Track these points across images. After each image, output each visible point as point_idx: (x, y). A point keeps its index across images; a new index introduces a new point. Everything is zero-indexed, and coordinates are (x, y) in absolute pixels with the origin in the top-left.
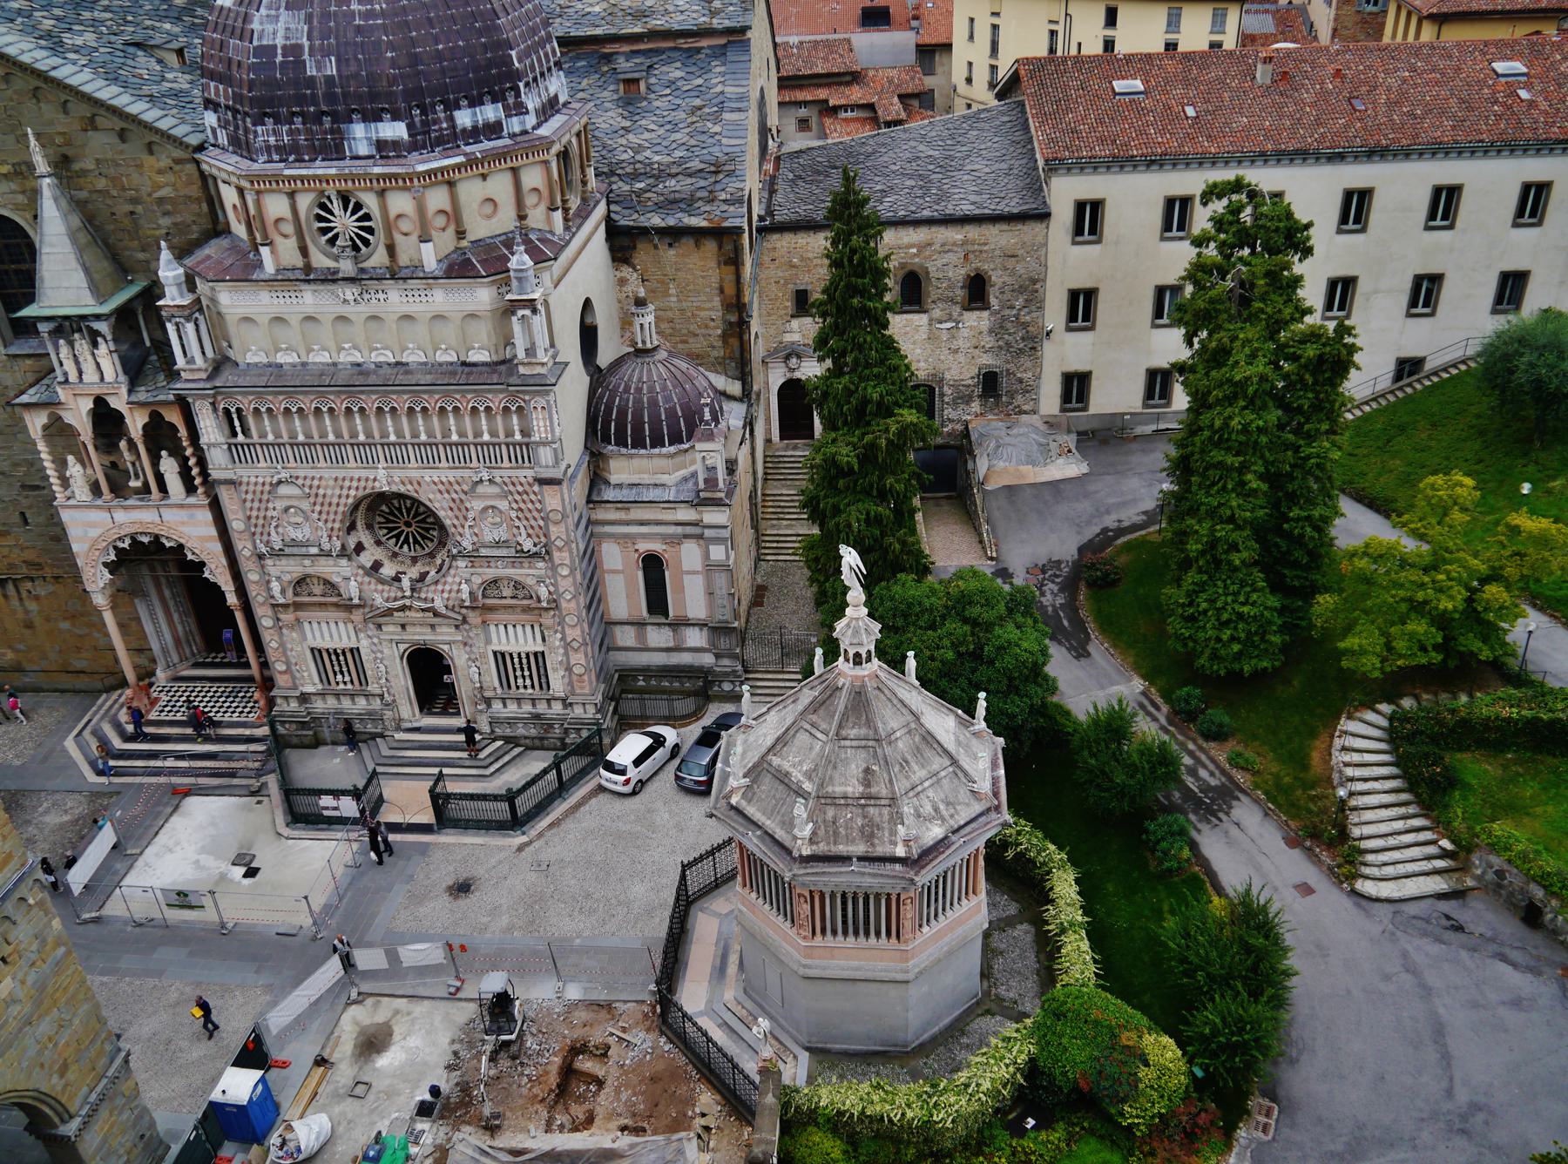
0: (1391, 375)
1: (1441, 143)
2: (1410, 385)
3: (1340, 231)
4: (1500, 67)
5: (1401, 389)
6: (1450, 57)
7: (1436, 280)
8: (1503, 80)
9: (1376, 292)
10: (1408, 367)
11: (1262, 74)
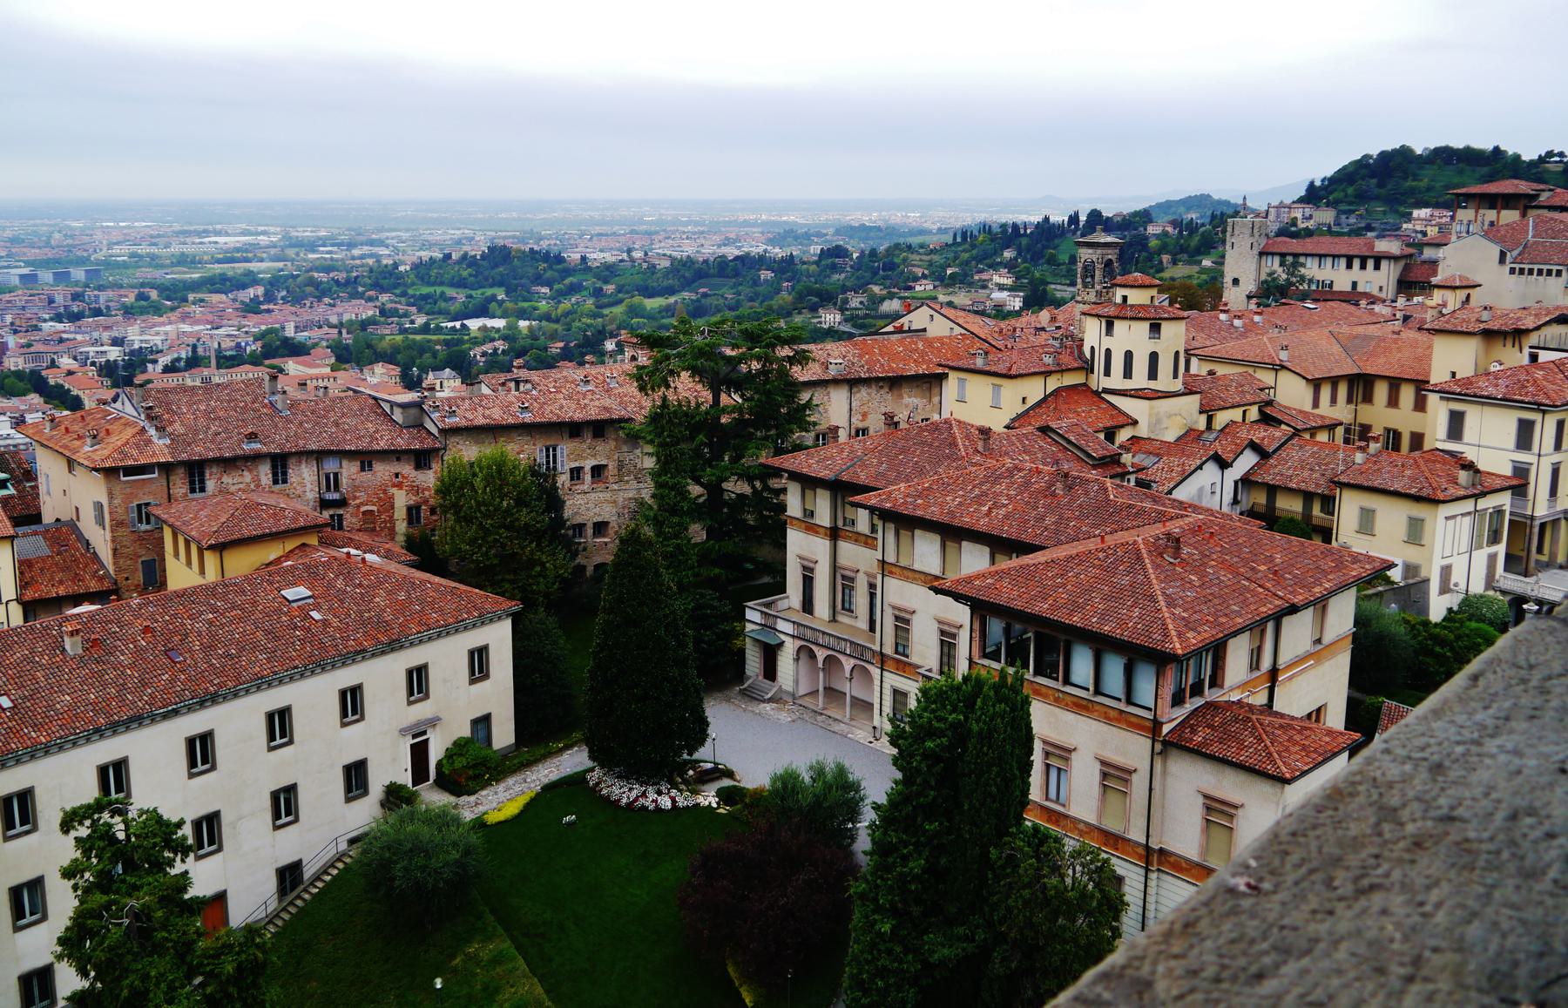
0: (276, 895)
1: (262, 677)
2: (299, 897)
3: (191, 776)
4: (290, 593)
5: (291, 903)
6: (243, 592)
7: (291, 790)
8: (295, 605)
9: (240, 818)
10: (289, 876)
11: (73, 645)
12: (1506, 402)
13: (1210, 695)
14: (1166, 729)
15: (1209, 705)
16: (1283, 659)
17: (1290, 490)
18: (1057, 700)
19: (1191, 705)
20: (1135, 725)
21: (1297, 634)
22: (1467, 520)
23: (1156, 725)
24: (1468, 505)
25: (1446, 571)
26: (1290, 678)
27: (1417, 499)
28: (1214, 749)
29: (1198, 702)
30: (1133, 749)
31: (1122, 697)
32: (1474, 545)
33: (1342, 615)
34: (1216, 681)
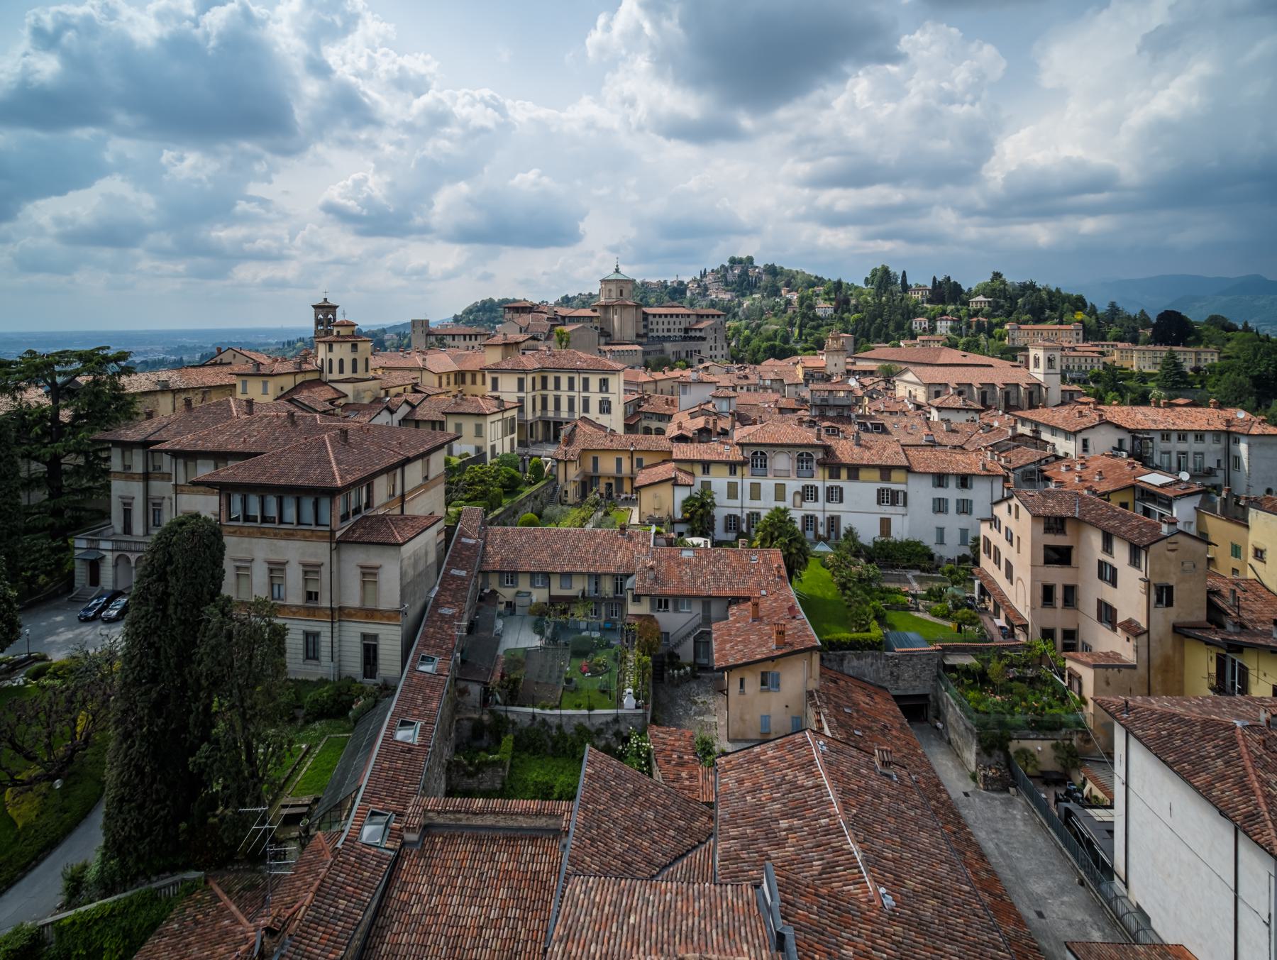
12: (512, 371)
13: (364, 513)
14: (338, 534)
15: (366, 517)
16: (407, 489)
17: (425, 421)
18: (275, 535)
19: (352, 520)
20: (321, 538)
21: (414, 473)
22: (500, 423)
23: (332, 532)
24: (499, 416)
25: (493, 447)
26: (412, 499)
27: (478, 415)
28: (365, 539)
29: (359, 516)
30: (319, 552)
31: (313, 522)
32: (504, 435)
33: (437, 463)
34: (368, 505)
